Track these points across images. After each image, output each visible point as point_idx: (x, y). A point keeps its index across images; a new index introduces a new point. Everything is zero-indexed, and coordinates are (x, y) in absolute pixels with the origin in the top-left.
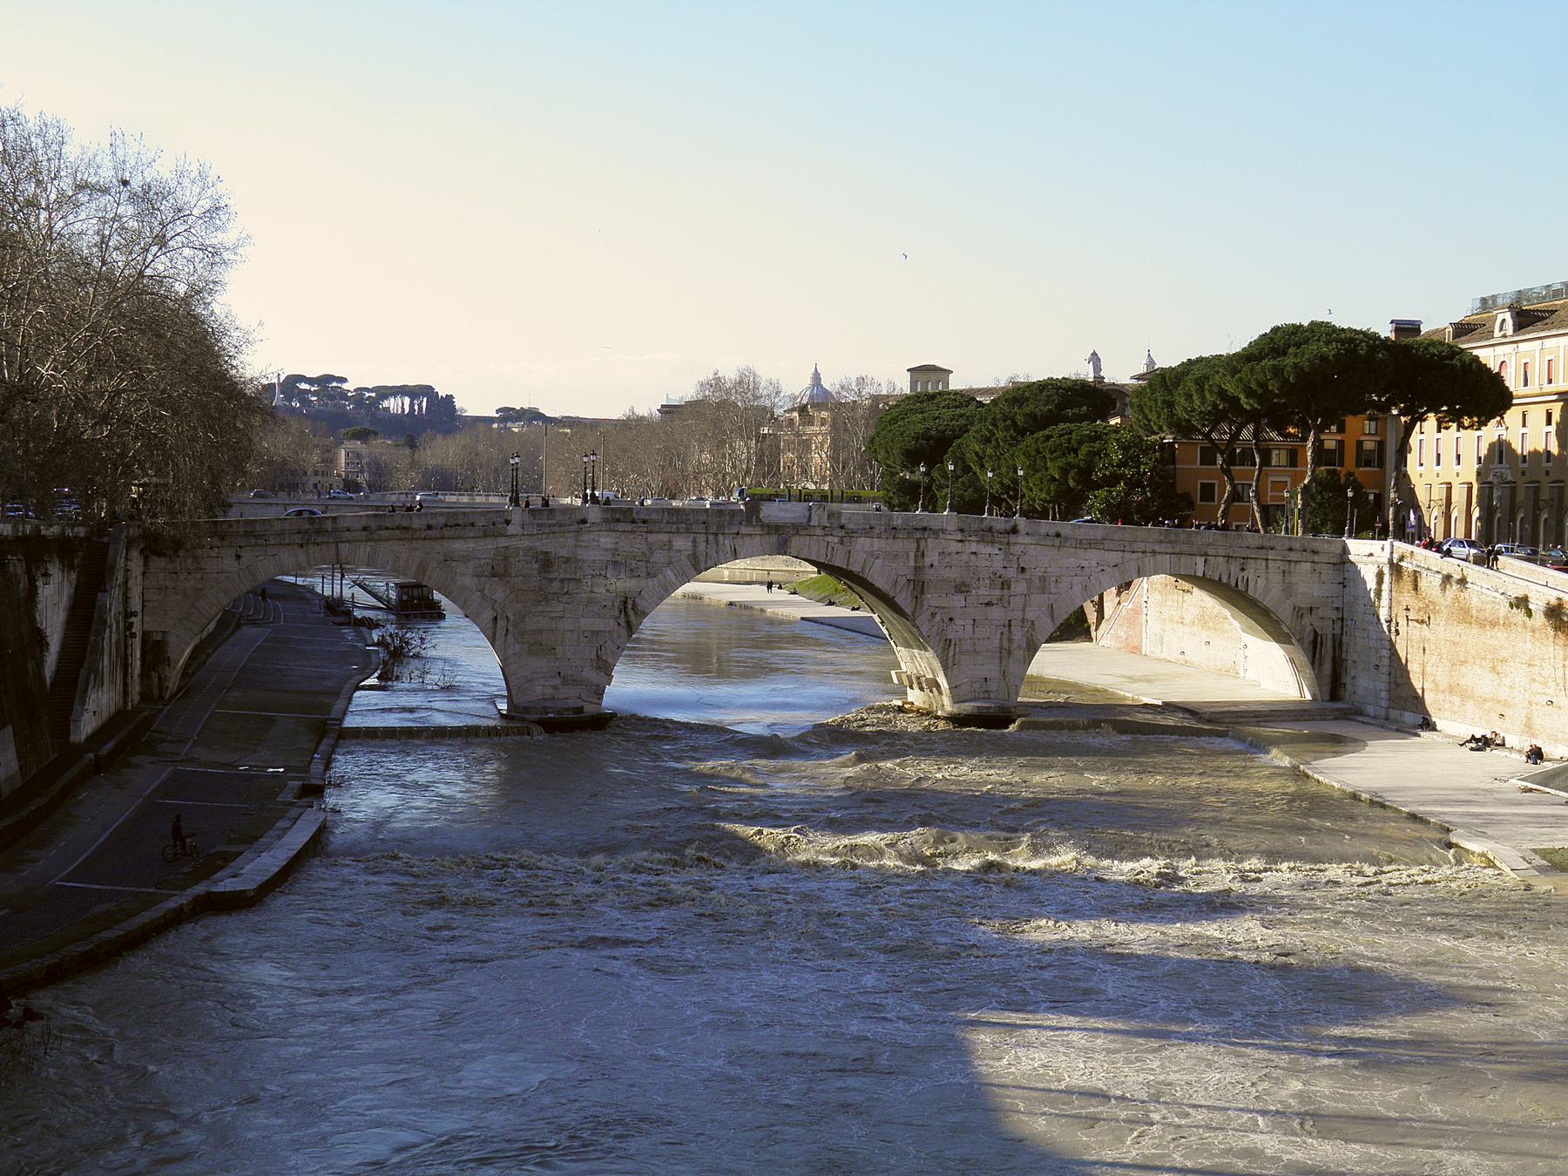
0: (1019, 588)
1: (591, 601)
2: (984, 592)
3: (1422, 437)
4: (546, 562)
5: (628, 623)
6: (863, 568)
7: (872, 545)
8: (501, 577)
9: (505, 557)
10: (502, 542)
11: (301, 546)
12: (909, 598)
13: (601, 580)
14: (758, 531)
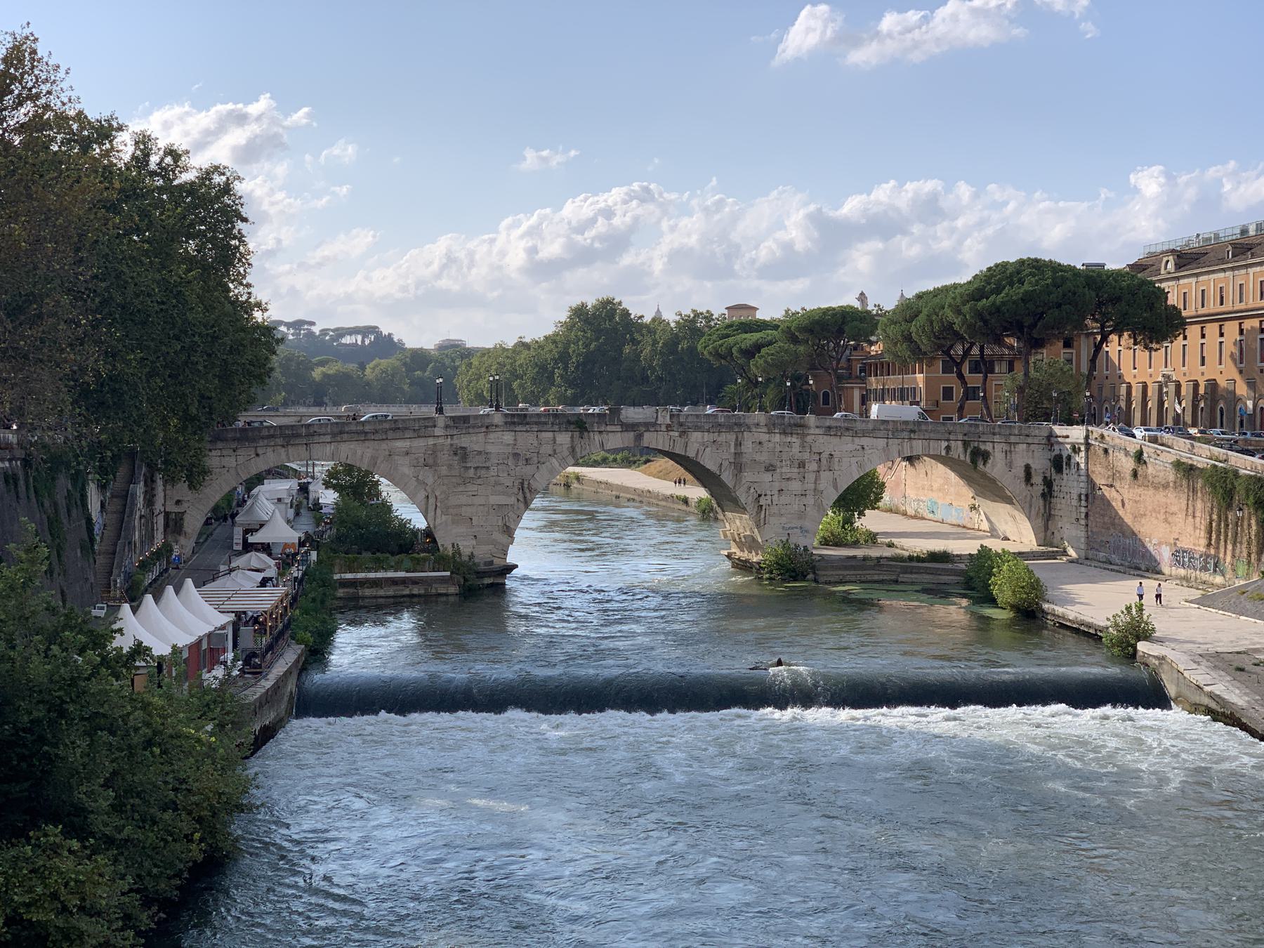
0: (813, 466)
1: (497, 484)
3: (1185, 343)
4: (462, 454)
5: (525, 498)
6: (697, 454)
8: (431, 467)
9: (434, 451)
10: (431, 441)
11: (283, 446)
13: (504, 467)
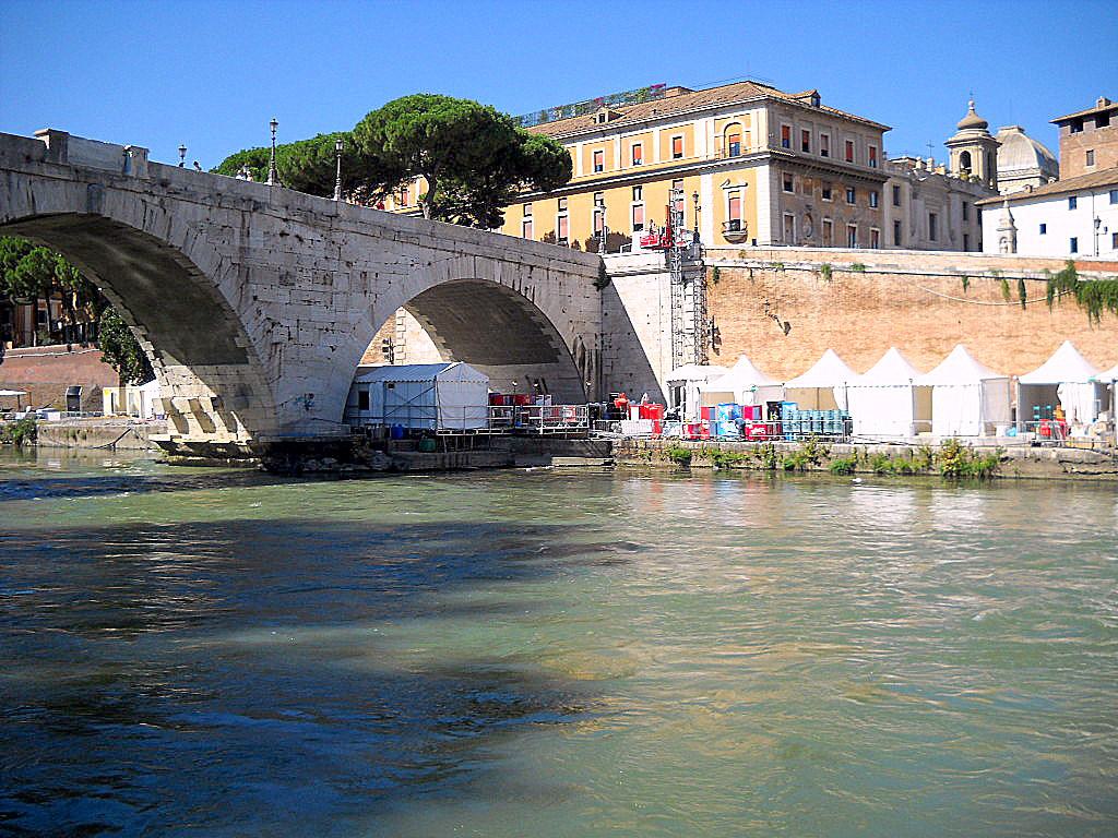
0: (341, 284)
7: (195, 213)
12: (234, 288)
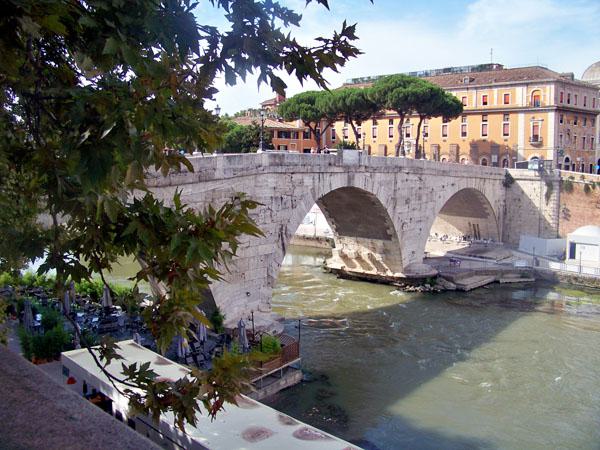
2: (414, 202)
10: (210, 186)
14: (341, 170)
